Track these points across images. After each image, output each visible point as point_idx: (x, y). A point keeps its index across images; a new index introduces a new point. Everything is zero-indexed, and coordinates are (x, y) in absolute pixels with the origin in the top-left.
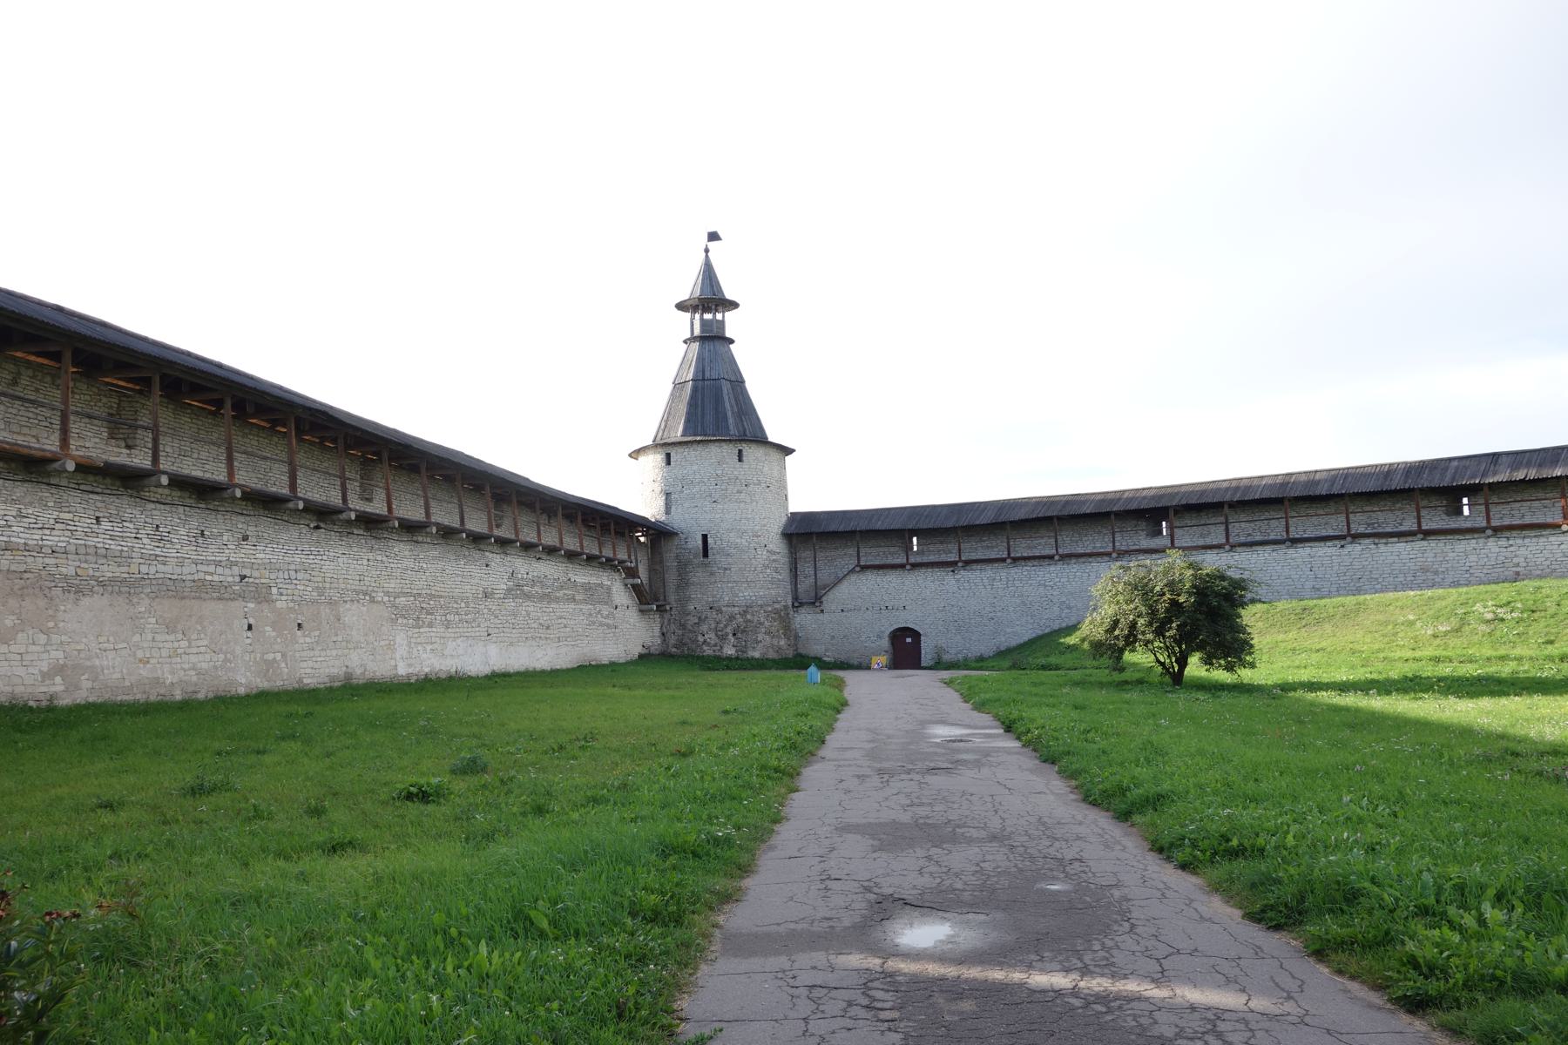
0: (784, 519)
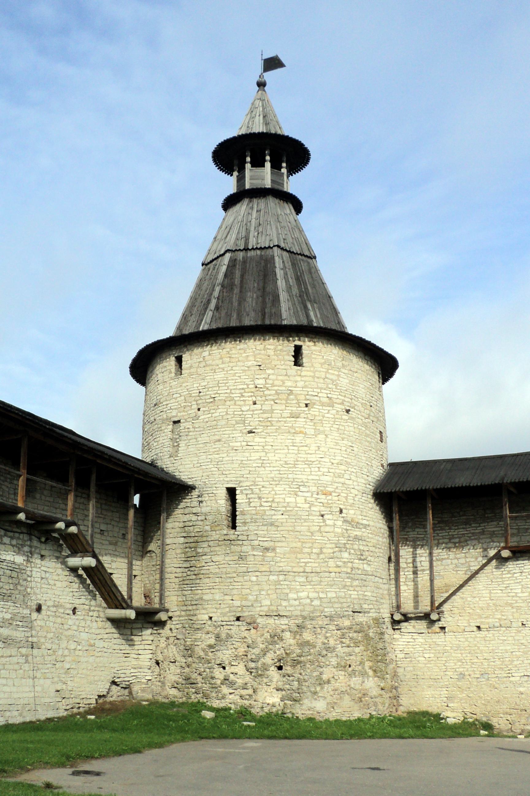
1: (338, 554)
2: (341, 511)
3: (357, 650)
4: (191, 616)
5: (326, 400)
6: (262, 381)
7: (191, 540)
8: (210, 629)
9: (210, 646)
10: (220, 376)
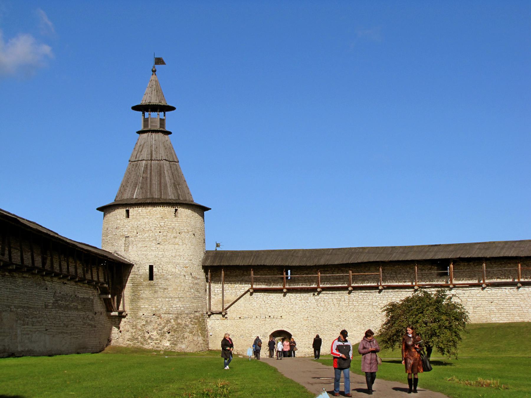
0: (202, 255)
2: (191, 274)
5: (186, 231)
6: (163, 224)
9: (144, 325)
10: (146, 220)
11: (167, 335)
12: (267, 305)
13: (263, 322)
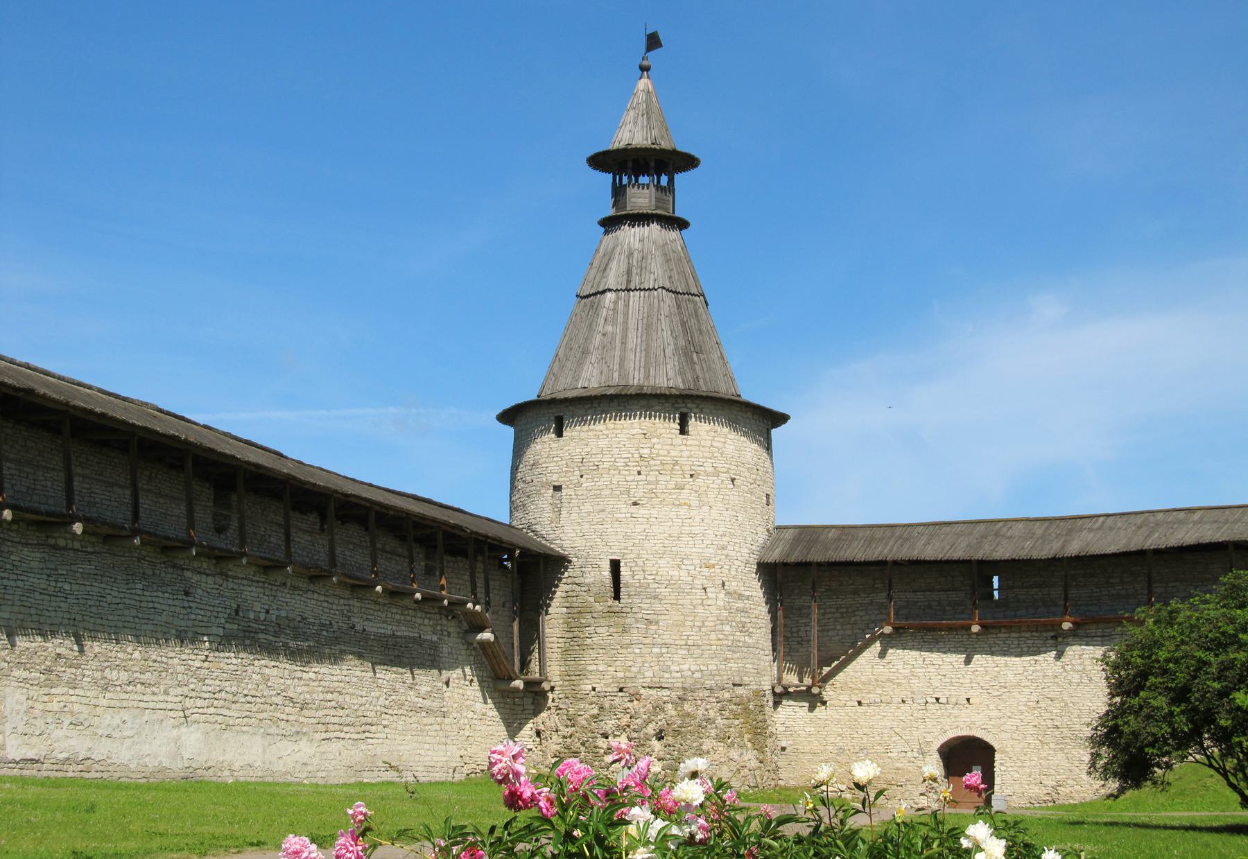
0: (762, 536)
1: (719, 627)
2: (723, 584)
3: (737, 722)
4: (574, 687)
5: (710, 470)
7: (575, 610)
8: (594, 699)
9: (594, 716)
10: (603, 443)
11: (656, 745)
12: (931, 669)
13: (920, 714)
